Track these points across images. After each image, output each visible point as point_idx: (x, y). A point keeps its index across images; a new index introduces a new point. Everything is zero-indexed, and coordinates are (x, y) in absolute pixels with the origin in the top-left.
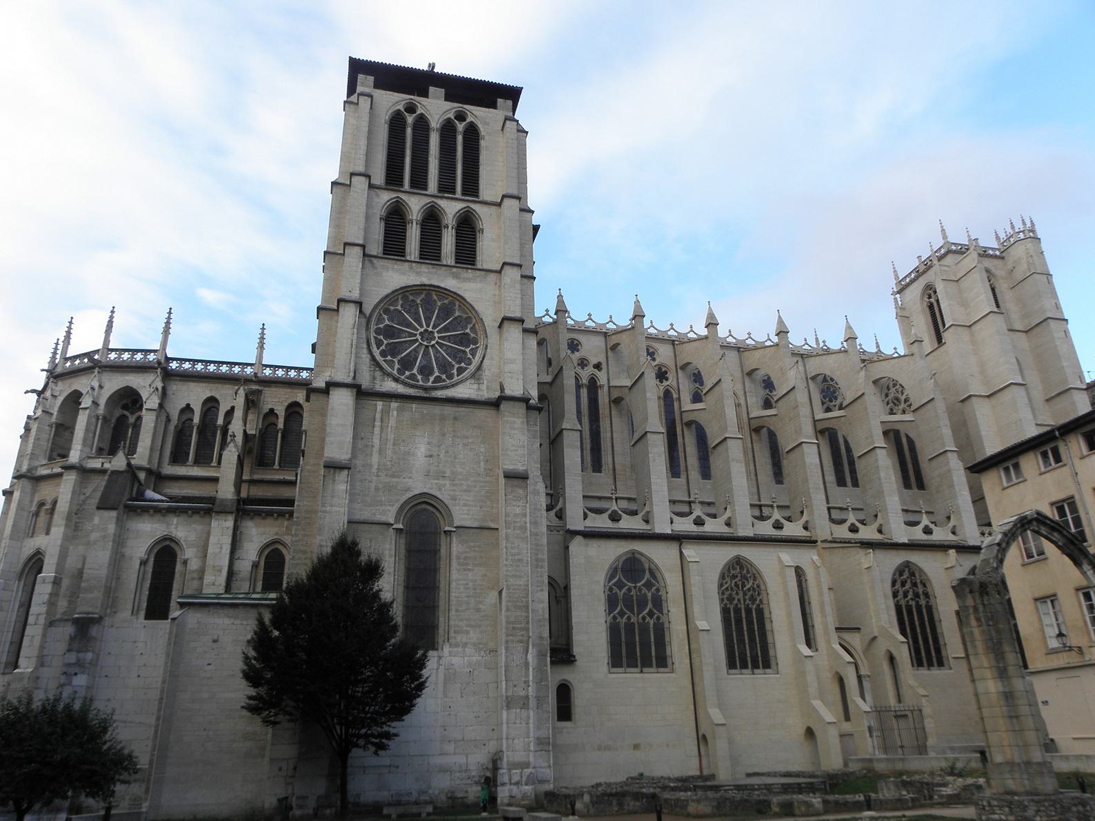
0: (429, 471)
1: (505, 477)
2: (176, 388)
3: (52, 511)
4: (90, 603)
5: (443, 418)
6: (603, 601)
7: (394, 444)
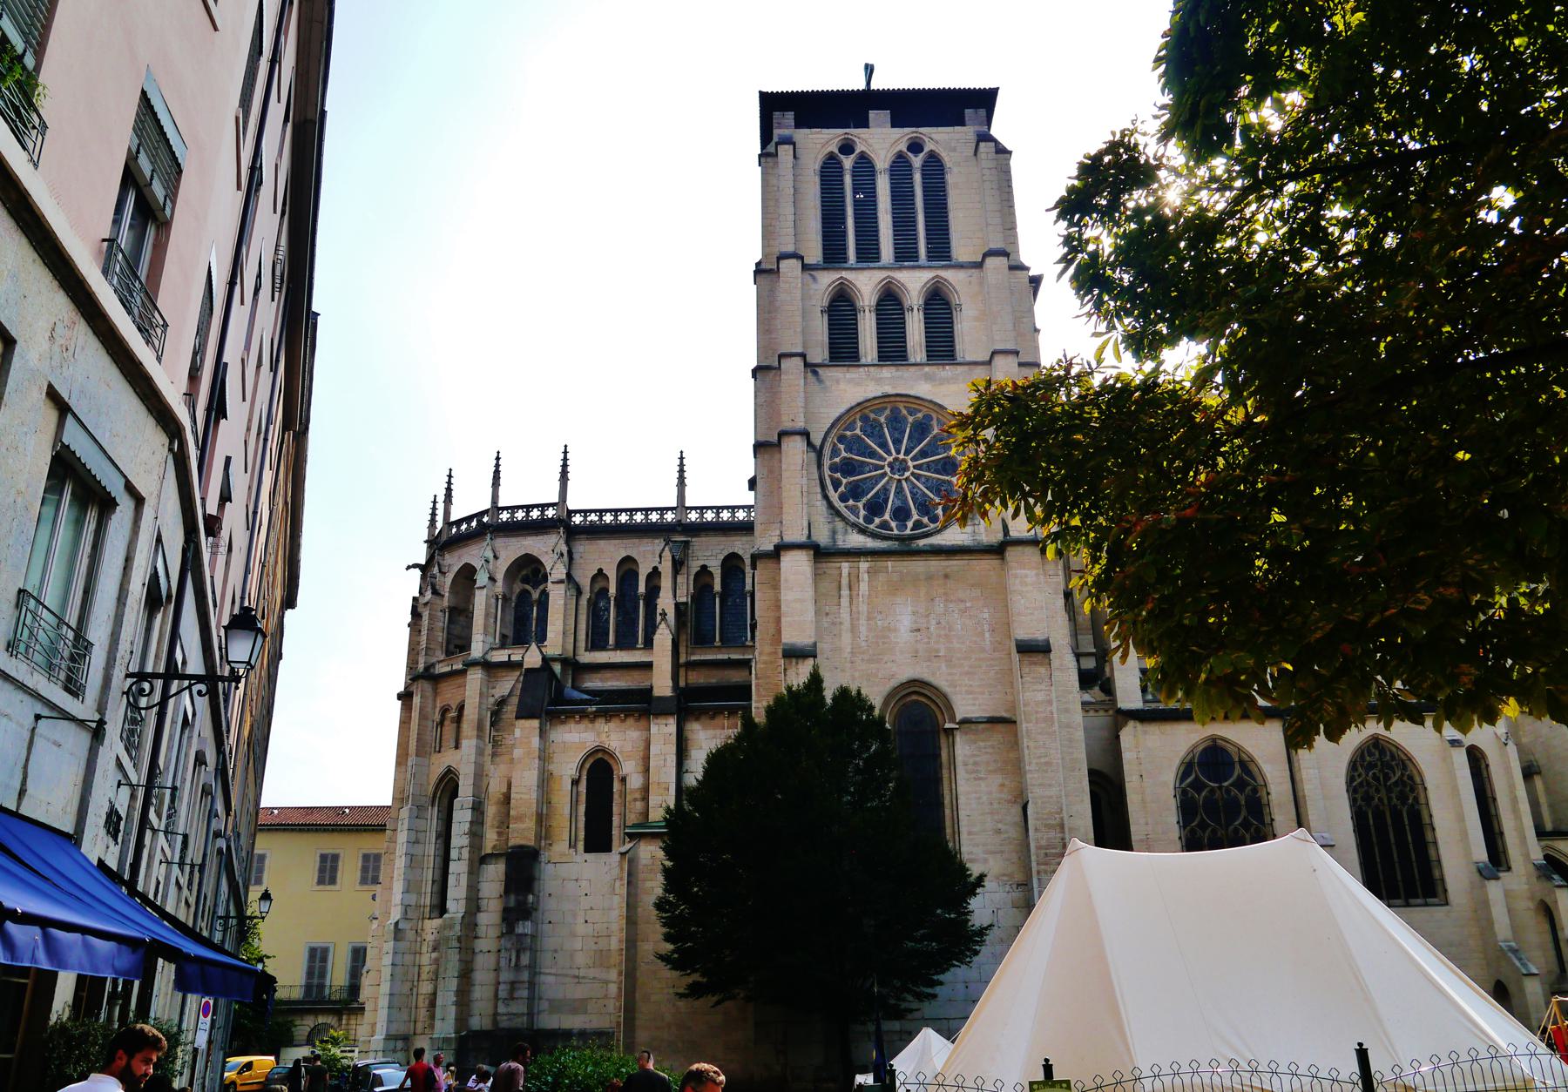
1: (1018, 652)
2: (583, 548)
3: (459, 719)
4: (523, 833)
5: (930, 578)
7: (869, 619)
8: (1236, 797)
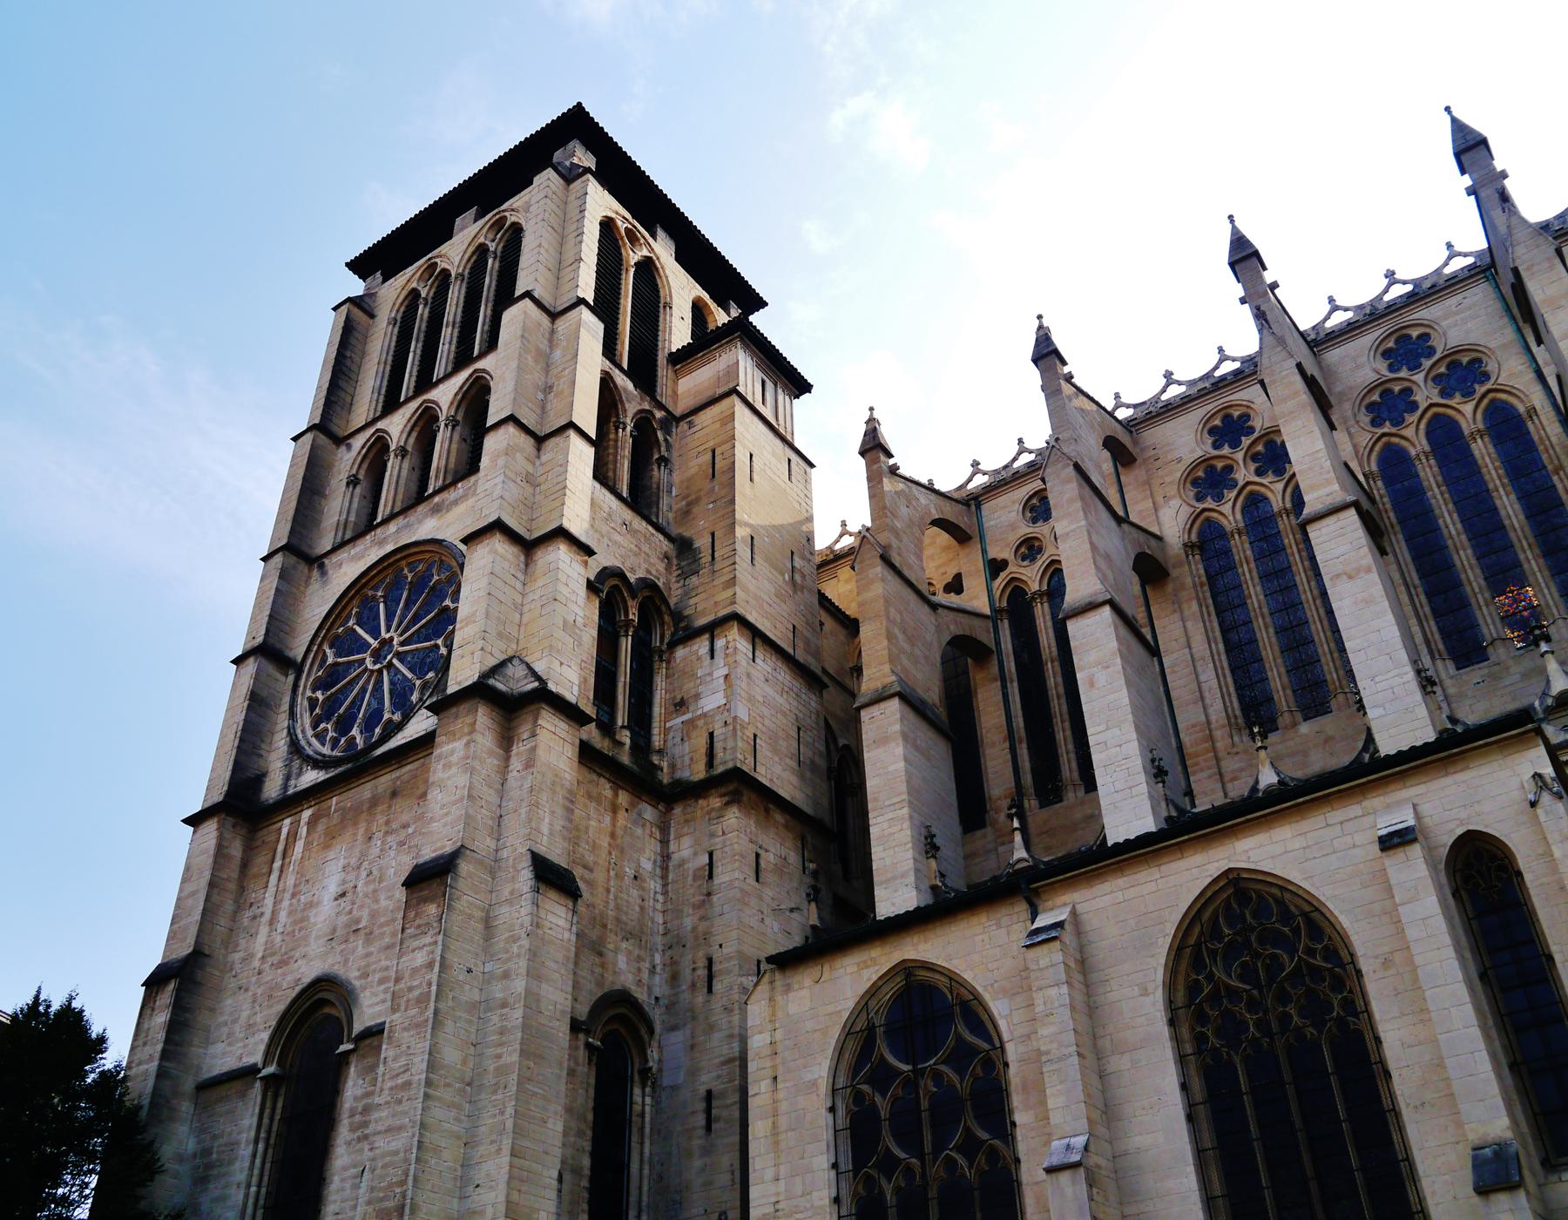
0: (334, 930)
5: (374, 802)
6: (826, 1135)
7: (293, 895)
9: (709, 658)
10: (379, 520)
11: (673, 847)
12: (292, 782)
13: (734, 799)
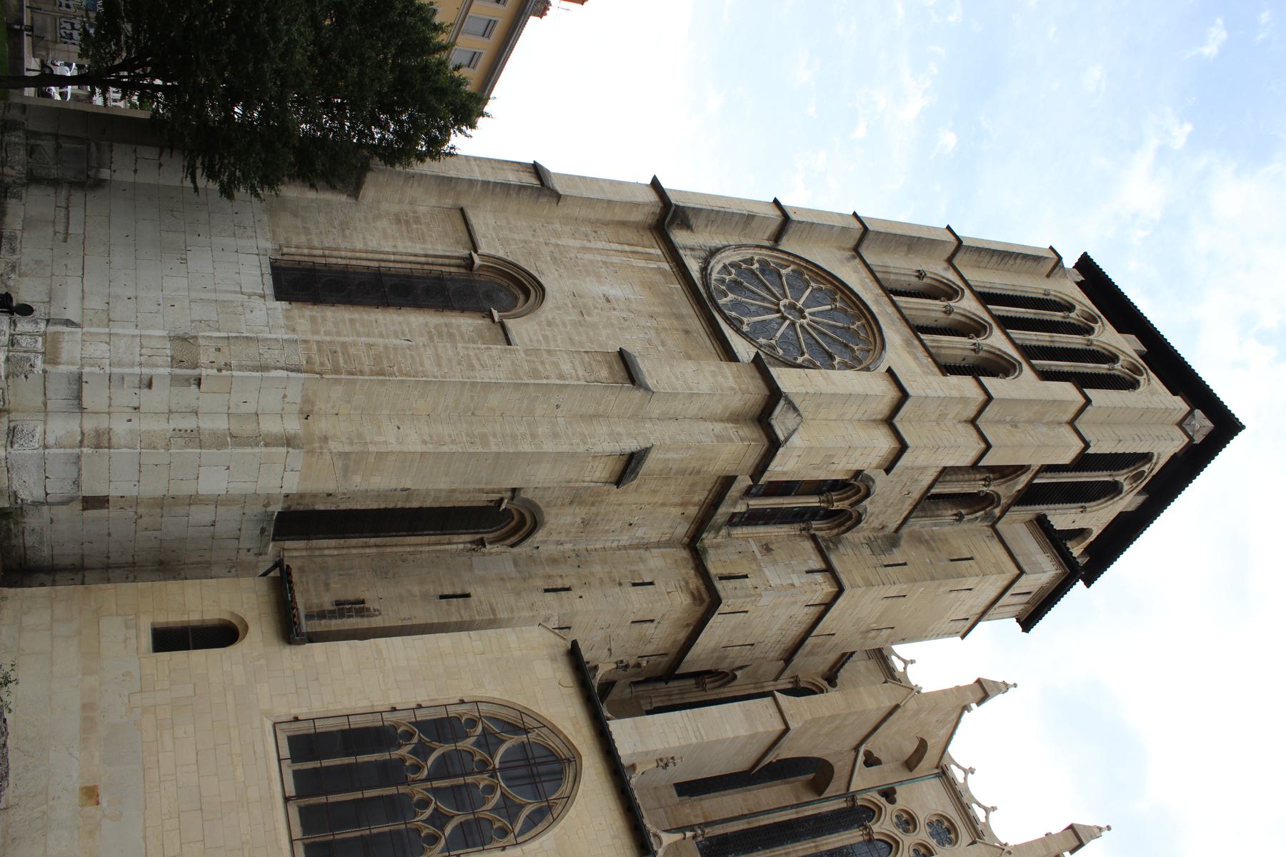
0: (581, 297)
5: (679, 317)
7: (605, 263)
8: (484, 802)
9: (807, 569)
10: (895, 298)
11: (656, 552)
12: (689, 252)
13: (696, 598)
